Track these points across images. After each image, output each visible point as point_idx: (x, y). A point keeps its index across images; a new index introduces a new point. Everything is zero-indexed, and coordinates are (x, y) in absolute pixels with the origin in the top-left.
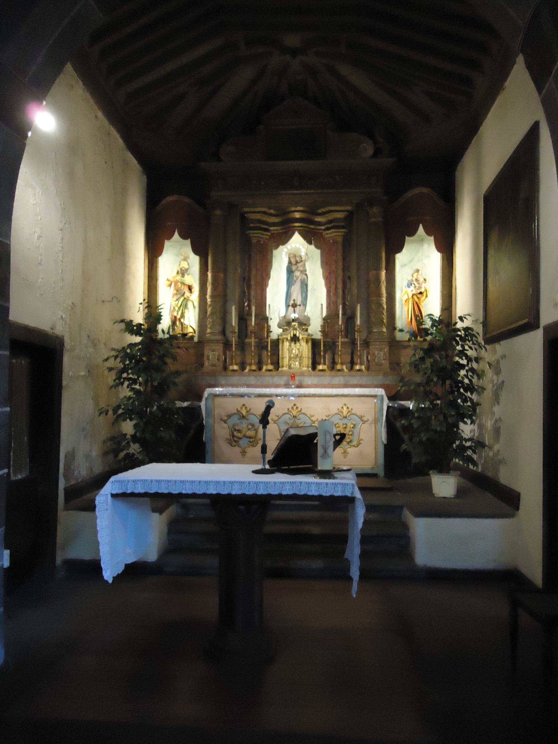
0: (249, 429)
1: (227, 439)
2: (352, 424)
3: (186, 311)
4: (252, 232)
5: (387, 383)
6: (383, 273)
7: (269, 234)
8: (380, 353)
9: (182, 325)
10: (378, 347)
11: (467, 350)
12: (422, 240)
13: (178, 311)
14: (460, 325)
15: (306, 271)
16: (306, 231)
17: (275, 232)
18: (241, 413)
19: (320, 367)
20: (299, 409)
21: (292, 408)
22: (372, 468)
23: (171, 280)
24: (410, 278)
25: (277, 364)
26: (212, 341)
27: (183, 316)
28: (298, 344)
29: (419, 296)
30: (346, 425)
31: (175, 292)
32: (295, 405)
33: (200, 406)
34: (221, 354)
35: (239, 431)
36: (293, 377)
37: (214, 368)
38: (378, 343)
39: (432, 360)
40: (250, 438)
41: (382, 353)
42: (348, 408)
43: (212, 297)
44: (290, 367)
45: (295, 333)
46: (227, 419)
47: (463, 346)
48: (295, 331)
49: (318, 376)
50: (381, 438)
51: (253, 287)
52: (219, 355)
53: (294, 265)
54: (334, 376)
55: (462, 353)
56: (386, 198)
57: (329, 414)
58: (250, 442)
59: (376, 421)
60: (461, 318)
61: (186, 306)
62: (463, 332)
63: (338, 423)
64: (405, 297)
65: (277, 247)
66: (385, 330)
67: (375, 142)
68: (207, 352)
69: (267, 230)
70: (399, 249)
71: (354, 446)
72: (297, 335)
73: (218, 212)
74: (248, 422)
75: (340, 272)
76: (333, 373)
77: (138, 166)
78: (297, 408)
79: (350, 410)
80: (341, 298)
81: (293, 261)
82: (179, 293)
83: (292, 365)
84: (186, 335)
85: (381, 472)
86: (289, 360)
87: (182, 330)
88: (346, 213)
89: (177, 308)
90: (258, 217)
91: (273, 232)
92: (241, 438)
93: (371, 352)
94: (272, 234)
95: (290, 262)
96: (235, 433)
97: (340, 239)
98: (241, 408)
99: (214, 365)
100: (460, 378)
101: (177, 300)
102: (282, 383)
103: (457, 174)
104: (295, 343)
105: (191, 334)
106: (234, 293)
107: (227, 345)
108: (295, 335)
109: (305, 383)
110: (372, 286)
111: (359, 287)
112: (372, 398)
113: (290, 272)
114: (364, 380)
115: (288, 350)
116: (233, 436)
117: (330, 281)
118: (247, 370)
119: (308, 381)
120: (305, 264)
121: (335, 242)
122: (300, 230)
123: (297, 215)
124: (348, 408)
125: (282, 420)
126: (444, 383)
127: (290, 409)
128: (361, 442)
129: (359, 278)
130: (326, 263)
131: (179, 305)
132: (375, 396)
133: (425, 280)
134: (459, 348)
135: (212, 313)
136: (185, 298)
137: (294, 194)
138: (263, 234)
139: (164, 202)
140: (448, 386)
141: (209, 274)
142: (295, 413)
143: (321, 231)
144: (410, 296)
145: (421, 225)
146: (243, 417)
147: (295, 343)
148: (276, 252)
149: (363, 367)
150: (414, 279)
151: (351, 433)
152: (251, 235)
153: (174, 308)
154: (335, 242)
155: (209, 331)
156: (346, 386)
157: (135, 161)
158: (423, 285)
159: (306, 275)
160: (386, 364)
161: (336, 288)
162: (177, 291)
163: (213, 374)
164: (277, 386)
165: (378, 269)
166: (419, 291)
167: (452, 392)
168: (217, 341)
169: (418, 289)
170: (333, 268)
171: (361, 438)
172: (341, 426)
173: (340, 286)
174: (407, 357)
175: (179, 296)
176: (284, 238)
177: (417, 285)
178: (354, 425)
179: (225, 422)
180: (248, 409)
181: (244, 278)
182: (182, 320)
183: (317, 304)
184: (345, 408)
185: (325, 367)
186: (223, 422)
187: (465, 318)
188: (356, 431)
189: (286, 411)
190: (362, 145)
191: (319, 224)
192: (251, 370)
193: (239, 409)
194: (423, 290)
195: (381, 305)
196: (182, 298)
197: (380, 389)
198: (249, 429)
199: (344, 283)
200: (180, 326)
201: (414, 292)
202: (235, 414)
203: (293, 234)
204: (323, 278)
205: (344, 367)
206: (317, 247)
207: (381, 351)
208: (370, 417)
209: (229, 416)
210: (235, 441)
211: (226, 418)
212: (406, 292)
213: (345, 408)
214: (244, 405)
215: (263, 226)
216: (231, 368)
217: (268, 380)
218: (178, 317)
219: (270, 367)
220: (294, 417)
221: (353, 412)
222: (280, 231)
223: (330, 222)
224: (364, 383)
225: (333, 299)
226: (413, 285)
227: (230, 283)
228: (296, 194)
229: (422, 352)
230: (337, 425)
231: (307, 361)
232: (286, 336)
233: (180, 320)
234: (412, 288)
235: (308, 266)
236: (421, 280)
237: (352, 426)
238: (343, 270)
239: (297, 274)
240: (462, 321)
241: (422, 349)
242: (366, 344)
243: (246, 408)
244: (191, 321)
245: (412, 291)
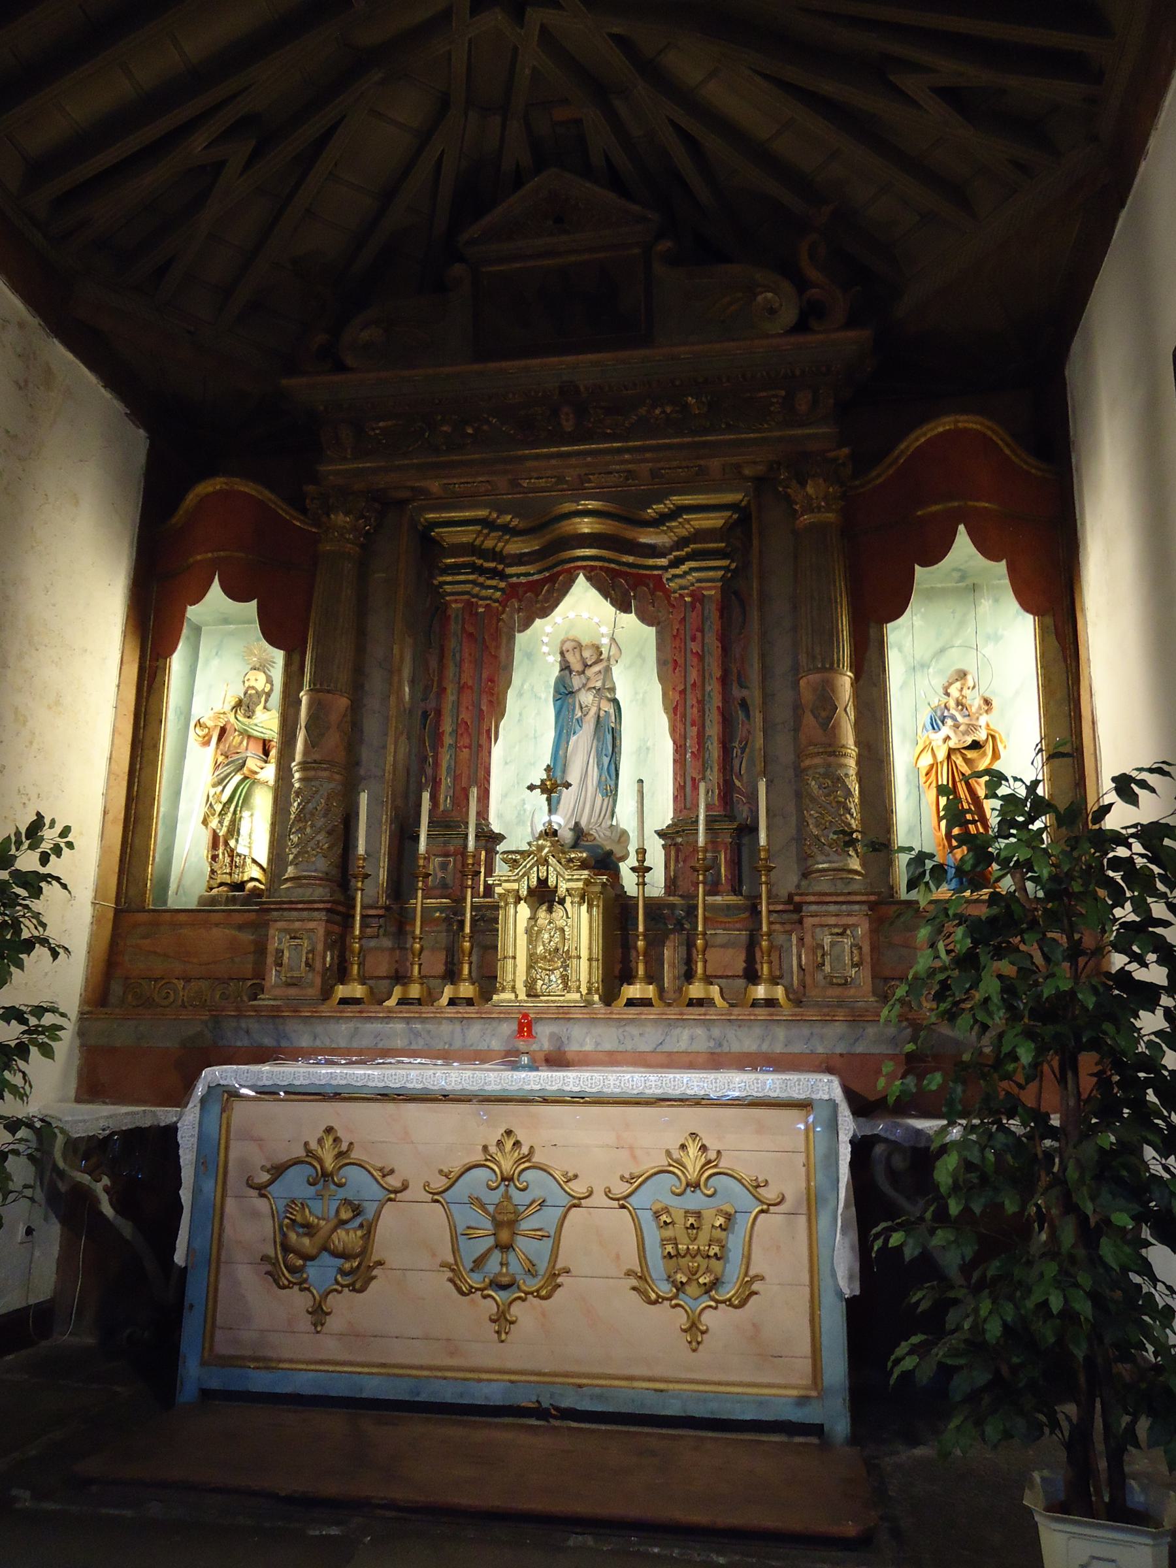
0: (343, 1223)
1: (265, 1258)
2: (720, 1212)
3: (246, 814)
4: (449, 579)
5: (860, 1049)
6: (845, 682)
7: (502, 585)
8: (840, 943)
9: (232, 857)
10: (832, 921)
11: (1166, 924)
12: (970, 589)
14: (1120, 817)
15: (613, 690)
16: (607, 570)
17: (523, 580)
18: (320, 1161)
19: (634, 991)
20: (525, 1150)
21: (499, 1143)
22: (802, 1401)
23: (210, 724)
24: (937, 699)
25: (488, 982)
26: (290, 905)
28: (559, 911)
29: (970, 754)
30: (698, 1215)
31: (221, 759)
32: (509, 1133)
33: (172, 1130)
34: (320, 947)
35: (309, 1229)
36: (525, 1026)
37: (292, 991)
38: (832, 908)
39: (1006, 967)
40: (344, 1255)
41: (847, 942)
42: (704, 1148)
43: (304, 766)
44: (532, 993)
45: (543, 875)
46: (271, 1182)
47: (1140, 907)
48: (543, 869)
49: (621, 1022)
50: (834, 1275)
51: (448, 740)
52: (312, 951)
53: (579, 672)
54: (671, 1024)
55: (1142, 934)
56: (845, 451)
57: (636, 1172)
58: (342, 1272)
59: (813, 1202)
60: (1125, 786)
61: (246, 801)
62: (1137, 847)
63: (666, 1210)
64: (926, 761)
65: (527, 624)
66: (855, 864)
67: (802, 285)
68: (276, 940)
69: (503, 576)
70: (897, 611)
71: (728, 1302)
72: (552, 882)
73: (340, 519)
74: (342, 1193)
75: (713, 688)
76: (672, 1013)
77: (107, 395)
78: (517, 1144)
79: (712, 1155)
80: (716, 768)
81: (574, 661)
82: (231, 764)
83: (540, 983)
84: (240, 886)
85: (837, 1420)
86: (530, 967)
88: (729, 514)
89: (218, 807)
90: (465, 535)
91: (514, 580)
92: (312, 1258)
93: (808, 939)
94: (513, 586)
95: (566, 667)
96: (293, 1236)
97: (712, 592)
98: (320, 1141)
99: (292, 983)
100: (1142, 1048)
101: (220, 782)
102: (496, 1045)
103: (1073, 372)
104: (550, 910)
105: (250, 885)
106: (387, 752)
107: (340, 914)
108: (543, 882)
109: (573, 1048)
110: (809, 720)
111: (768, 729)
112: (794, 1113)
113: (564, 693)
114: (779, 1041)
115: (528, 931)
116: (286, 1248)
117: (684, 716)
118: (391, 1002)
119: (582, 1039)
120: (608, 670)
121: (698, 598)
122: (593, 568)
123: (586, 526)
124: (704, 1148)
125: (461, 1190)
126: (1069, 1065)
127: (493, 1149)
128: (755, 1287)
129: (767, 697)
130: (671, 665)
131: (225, 797)
132: (804, 1105)
133: (987, 702)
134: (1125, 913)
135: (298, 819)
136: (246, 778)
137: (560, 455)
138: (483, 586)
139: (191, 499)
140: (1087, 1083)
141: (304, 698)
142: (507, 1165)
143: (656, 572)
144: (941, 754)
145: (961, 528)
146: (326, 1175)
147: (550, 910)
148: (521, 639)
149: (779, 992)
150: (952, 704)
151: (715, 1249)
152: (448, 588)
154: (698, 598)
155: (291, 871)
156: (716, 1061)
157: (91, 378)
158: (983, 720)
159: (616, 702)
160: (863, 977)
161: (701, 738)
163: (274, 1015)
164: (479, 1057)
165: (831, 667)
166: (969, 740)
167: (1108, 1111)
168: (309, 906)
169: (966, 733)
170: (693, 675)
171: (752, 1273)
172: (679, 1216)
173: (713, 730)
174: (927, 955)
175: (228, 769)
176: (543, 596)
177: (960, 719)
178: (729, 1217)
179: (261, 1190)
180: (344, 1147)
181: (425, 715)
182: (232, 843)
183: (647, 790)
184: (693, 1150)
185: (650, 991)
186: (255, 1193)
187: (1143, 784)
188: (736, 1243)
189: (479, 1157)
190: (760, 298)
191: (653, 551)
192: (403, 1002)
193: (313, 1145)
194: (981, 736)
195: (839, 781)
196: (239, 777)
197: (826, 1078)
198: (343, 1223)
199: (727, 721)
200: (227, 860)
201: (952, 744)
202: (297, 1162)
203: (571, 581)
204: (665, 709)
205: (715, 991)
206: (644, 618)
207: (842, 934)
208: (789, 1184)
209: (278, 1171)
210: (293, 1270)
211: (265, 1177)
212: (929, 747)
213: (693, 1150)
214: (329, 1130)
215: (488, 563)
216: (341, 991)
217: (447, 1033)
218: (222, 833)
219: (466, 990)
220: (503, 1179)
221: (724, 1164)
222: (536, 577)
223: (682, 542)
224: (779, 1048)
225: (692, 772)
226: (949, 722)
227: (371, 726)
228: (569, 455)
229: (960, 932)
230: (664, 1218)
231: (585, 971)
232: (515, 886)
233: (226, 844)
234: (946, 730)
235: (617, 672)
236: (975, 703)
237: (720, 1221)
238: (724, 680)
239: (586, 698)
240: (1132, 799)
241: (961, 919)
242: (794, 908)
243: (337, 1140)
244: (255, 840)
245: (948, 738)
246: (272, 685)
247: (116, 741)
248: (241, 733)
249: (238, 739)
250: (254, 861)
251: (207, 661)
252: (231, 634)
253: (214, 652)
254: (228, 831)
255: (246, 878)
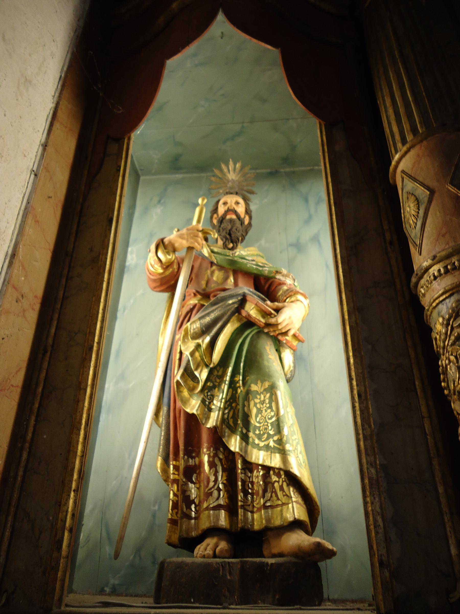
13: (209, 389)
27: (237, 417)
61: (253, 364)
87: (231, 509)
89: (203, 375)
153: (188, 373)
162: (206, 296)
246: (250, 218)
247: (30, 230)
248: (221, 268)
249: (217, 276)
250: (293, 481)
251: (146, 210)
252: (178, 182)
253: (156, 199)
254: (223, 420)
255: (277, 522)
